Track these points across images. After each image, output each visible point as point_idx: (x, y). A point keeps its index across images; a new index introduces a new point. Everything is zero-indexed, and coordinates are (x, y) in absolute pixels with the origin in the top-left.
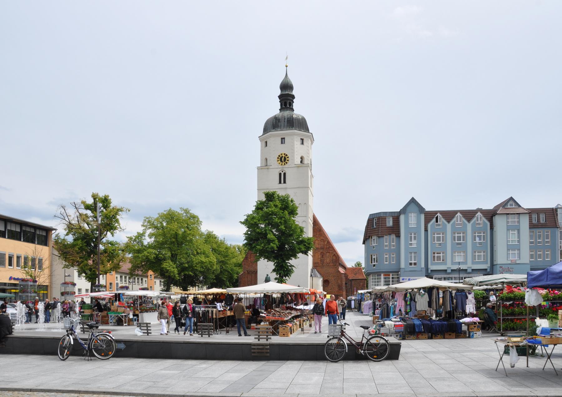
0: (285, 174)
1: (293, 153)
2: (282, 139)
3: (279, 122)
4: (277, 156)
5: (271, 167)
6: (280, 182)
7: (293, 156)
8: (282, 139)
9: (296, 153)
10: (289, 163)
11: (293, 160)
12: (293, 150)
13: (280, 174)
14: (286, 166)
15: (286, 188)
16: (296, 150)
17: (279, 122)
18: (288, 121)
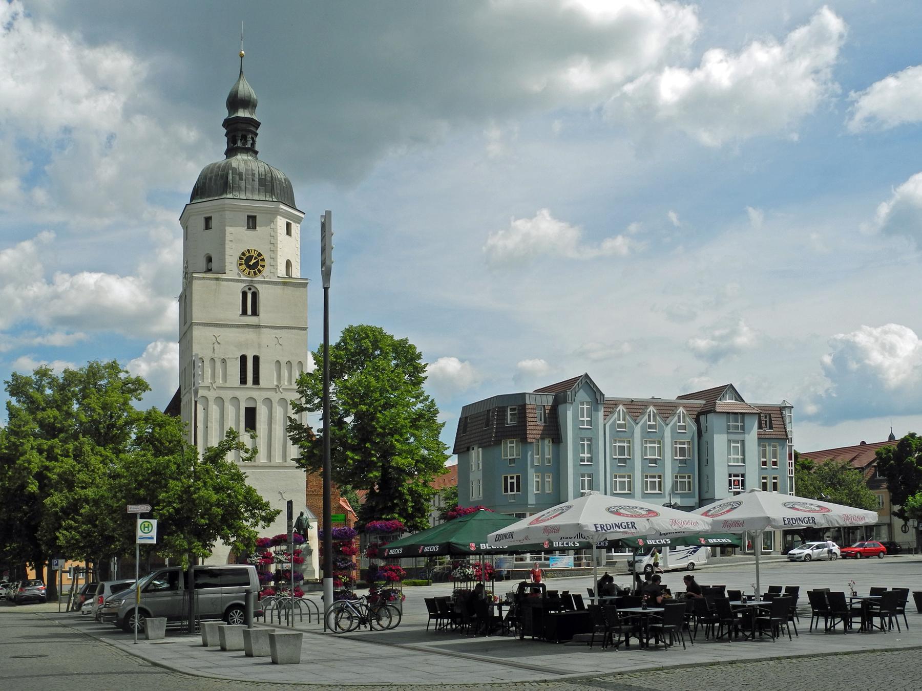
0: (255, 295)
1: (274, 251)
2: (249, 217)
3: (241, 179)
4: (239, 254)
5: (224, 276)
6: (244, 312)
7: (274, 259)
8: (249, 217)
9: (279, 253)
10: (265, 271)
11: (274, 266)
12: (273, 244)
13: (244, 294)
14: (259, 278)
15: (258, 326)
16: (279, 246)
17: (241, 179)
18: (259, 179)
